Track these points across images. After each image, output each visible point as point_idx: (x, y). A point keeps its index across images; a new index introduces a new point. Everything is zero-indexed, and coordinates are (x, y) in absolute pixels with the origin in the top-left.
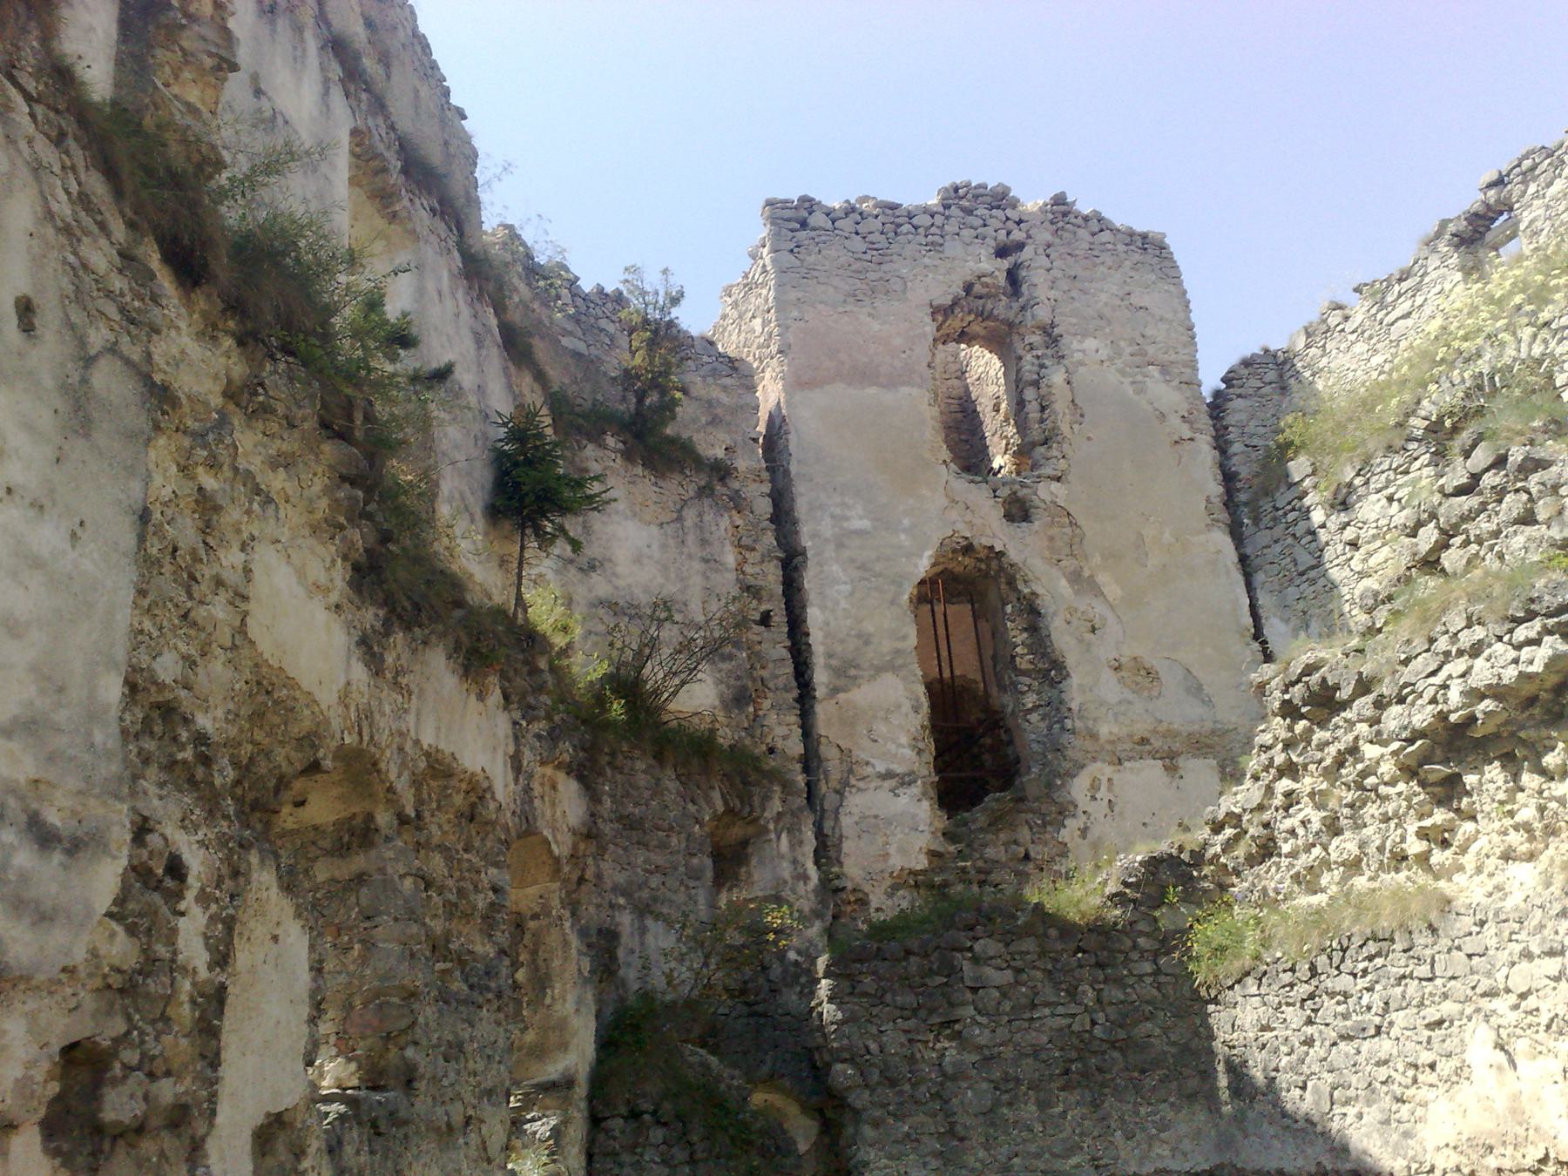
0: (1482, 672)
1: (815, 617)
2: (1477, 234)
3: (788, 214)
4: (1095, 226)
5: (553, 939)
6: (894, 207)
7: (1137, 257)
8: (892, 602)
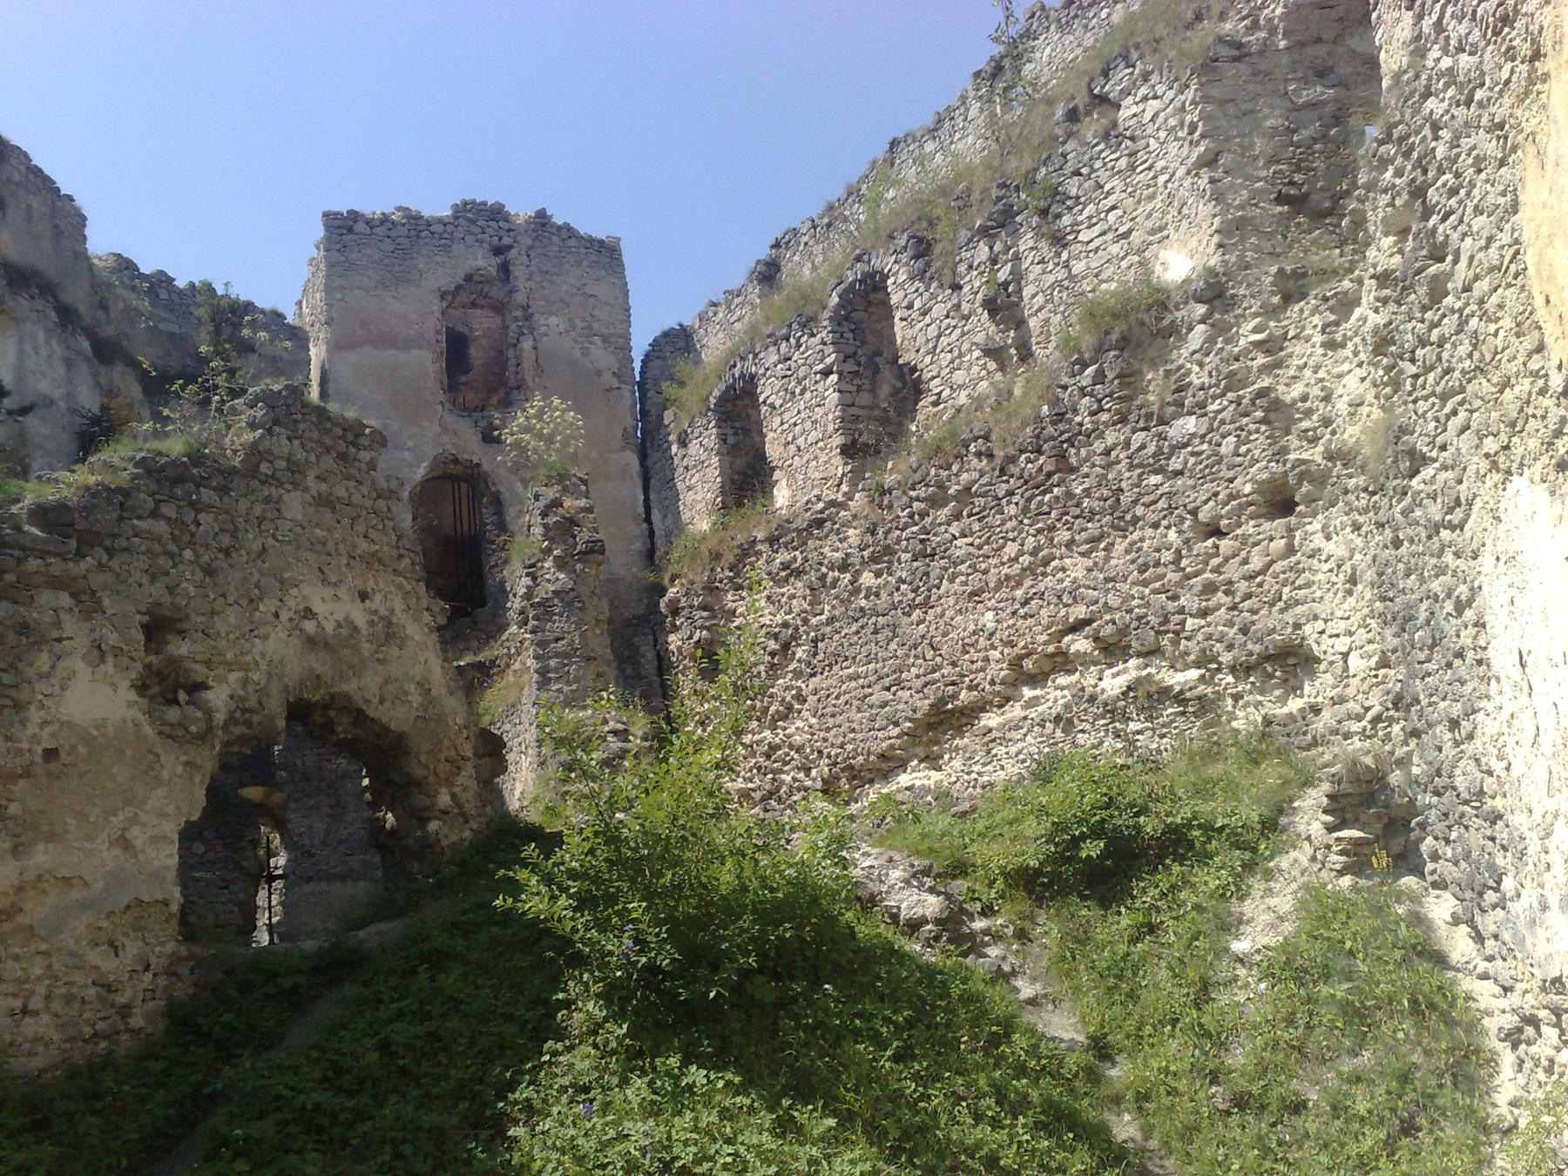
2: (768, 274)
4: (564, 234)
6: (419, 217)
7: (593, 258)
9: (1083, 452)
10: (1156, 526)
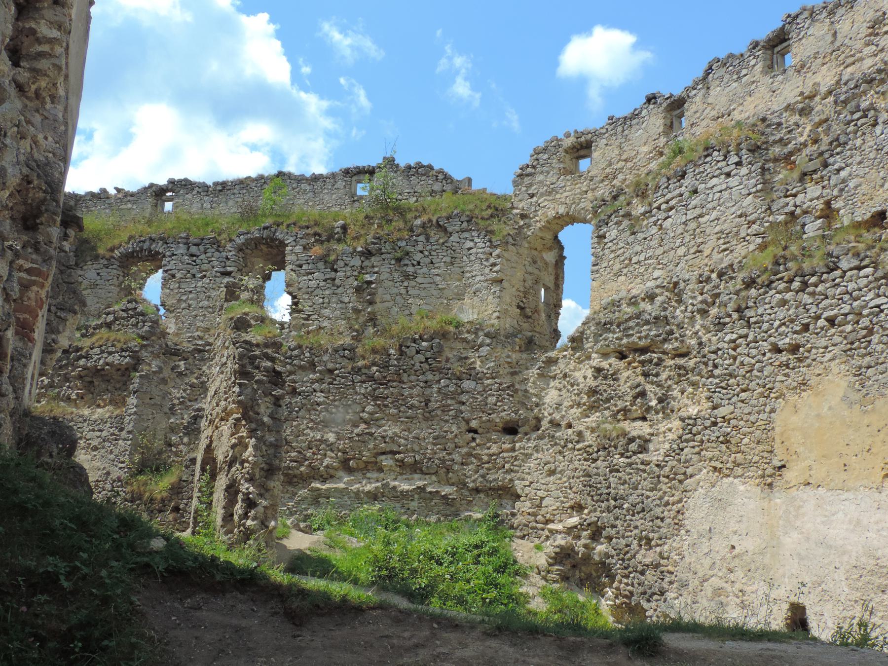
0: (110, 359)
9: (413, 378)
10: (447, 421)
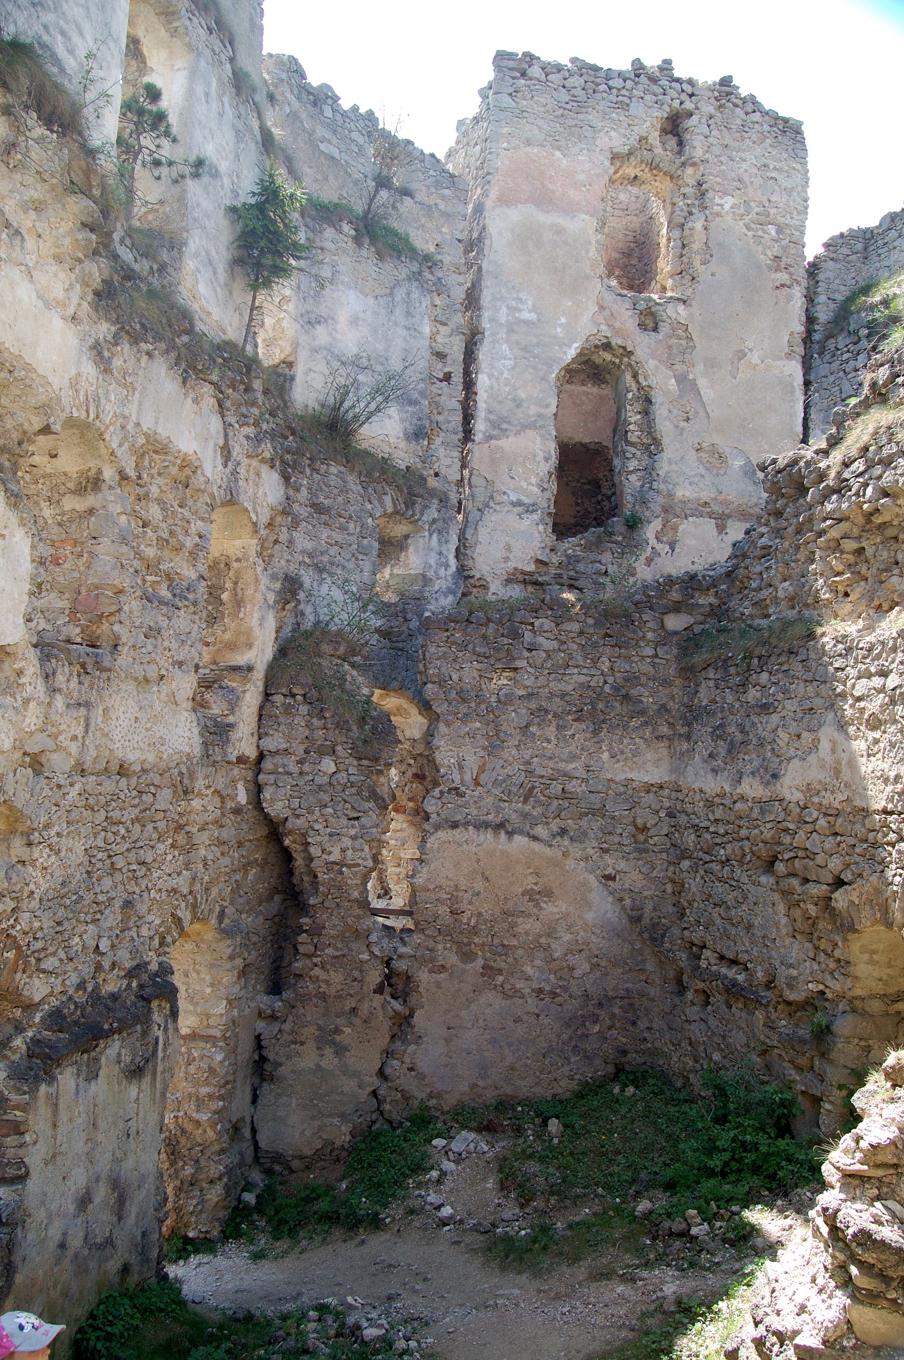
1: (483, 381)
3: (512, 64)
4: (750, 107)
5: (248, 576)
6: (595, 69)
8: (543, 378)
